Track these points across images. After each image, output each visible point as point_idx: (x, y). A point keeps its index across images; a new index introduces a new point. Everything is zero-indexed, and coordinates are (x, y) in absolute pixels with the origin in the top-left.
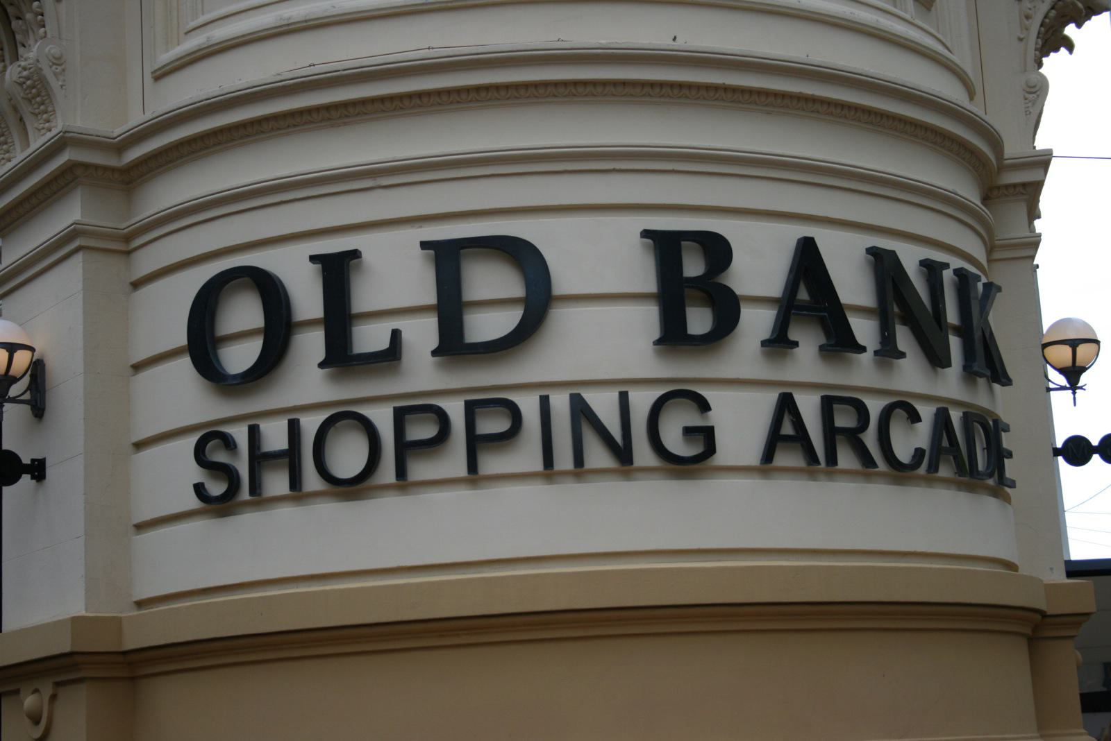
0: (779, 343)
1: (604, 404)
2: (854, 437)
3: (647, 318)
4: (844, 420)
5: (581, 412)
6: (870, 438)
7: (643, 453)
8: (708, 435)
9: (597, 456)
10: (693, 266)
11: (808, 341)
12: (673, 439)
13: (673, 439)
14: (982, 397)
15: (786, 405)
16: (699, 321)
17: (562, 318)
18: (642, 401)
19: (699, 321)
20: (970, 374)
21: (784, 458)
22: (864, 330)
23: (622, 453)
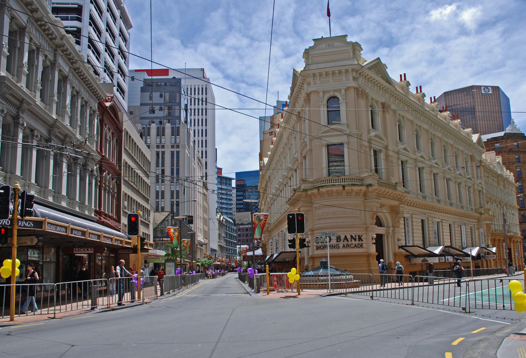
0: (344, 241)
1: (334, 245)
2: (348, 246)
3: (336, 240)
4: (348, 245)
5: (332, 245)
6: (350, 246)
7: (336, 248)
8: (339, 247)
9: (333, 248)
10: (339, 237)
11: (345, 241)
12: (337, 247)
13: (337, 247)
14: (361, 242)
15: (344, 245)
16: (339, 240)
17: (332, 241)
18: (336, 245)
19: (339, 240)
20: (359, 241)
21: (344, 248)
22: (349, 240)
23: (335, 248)
